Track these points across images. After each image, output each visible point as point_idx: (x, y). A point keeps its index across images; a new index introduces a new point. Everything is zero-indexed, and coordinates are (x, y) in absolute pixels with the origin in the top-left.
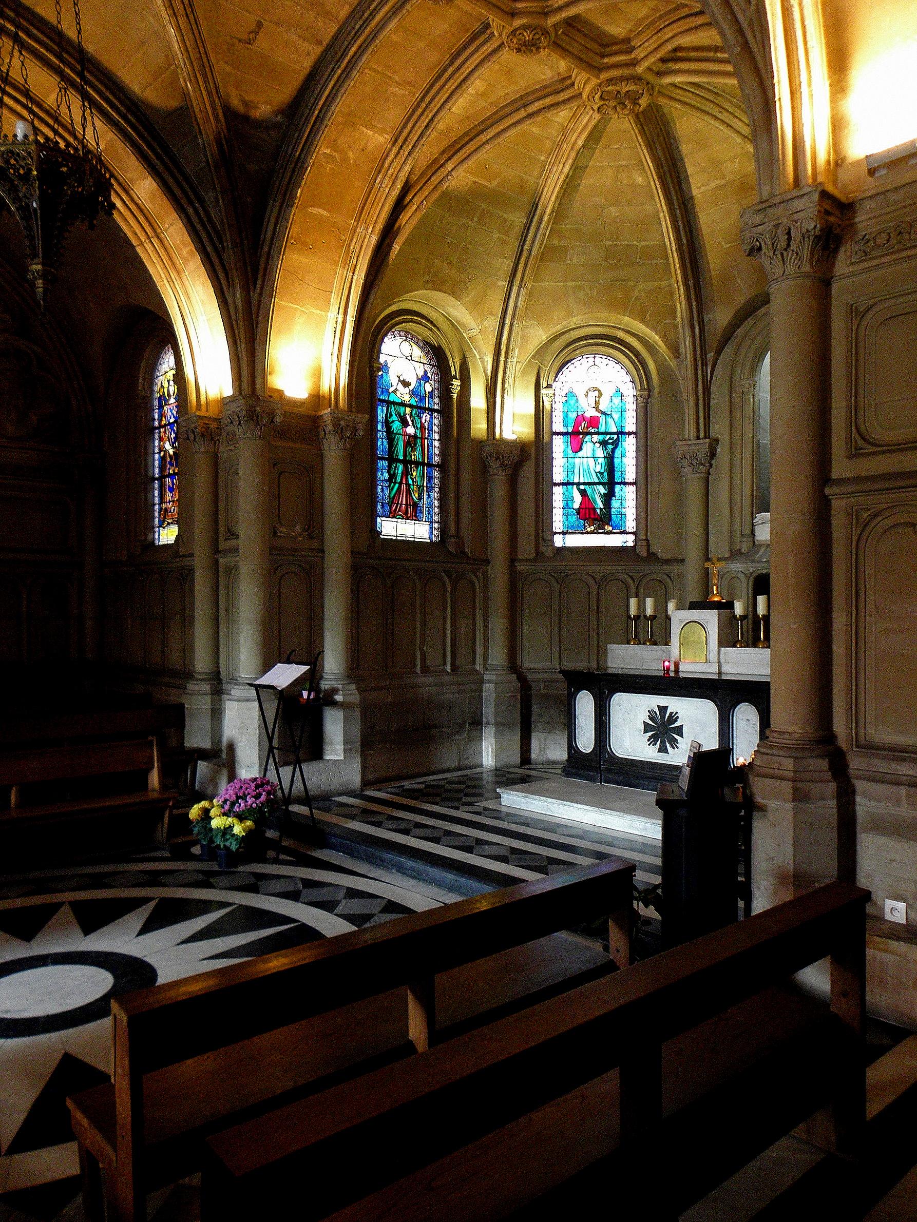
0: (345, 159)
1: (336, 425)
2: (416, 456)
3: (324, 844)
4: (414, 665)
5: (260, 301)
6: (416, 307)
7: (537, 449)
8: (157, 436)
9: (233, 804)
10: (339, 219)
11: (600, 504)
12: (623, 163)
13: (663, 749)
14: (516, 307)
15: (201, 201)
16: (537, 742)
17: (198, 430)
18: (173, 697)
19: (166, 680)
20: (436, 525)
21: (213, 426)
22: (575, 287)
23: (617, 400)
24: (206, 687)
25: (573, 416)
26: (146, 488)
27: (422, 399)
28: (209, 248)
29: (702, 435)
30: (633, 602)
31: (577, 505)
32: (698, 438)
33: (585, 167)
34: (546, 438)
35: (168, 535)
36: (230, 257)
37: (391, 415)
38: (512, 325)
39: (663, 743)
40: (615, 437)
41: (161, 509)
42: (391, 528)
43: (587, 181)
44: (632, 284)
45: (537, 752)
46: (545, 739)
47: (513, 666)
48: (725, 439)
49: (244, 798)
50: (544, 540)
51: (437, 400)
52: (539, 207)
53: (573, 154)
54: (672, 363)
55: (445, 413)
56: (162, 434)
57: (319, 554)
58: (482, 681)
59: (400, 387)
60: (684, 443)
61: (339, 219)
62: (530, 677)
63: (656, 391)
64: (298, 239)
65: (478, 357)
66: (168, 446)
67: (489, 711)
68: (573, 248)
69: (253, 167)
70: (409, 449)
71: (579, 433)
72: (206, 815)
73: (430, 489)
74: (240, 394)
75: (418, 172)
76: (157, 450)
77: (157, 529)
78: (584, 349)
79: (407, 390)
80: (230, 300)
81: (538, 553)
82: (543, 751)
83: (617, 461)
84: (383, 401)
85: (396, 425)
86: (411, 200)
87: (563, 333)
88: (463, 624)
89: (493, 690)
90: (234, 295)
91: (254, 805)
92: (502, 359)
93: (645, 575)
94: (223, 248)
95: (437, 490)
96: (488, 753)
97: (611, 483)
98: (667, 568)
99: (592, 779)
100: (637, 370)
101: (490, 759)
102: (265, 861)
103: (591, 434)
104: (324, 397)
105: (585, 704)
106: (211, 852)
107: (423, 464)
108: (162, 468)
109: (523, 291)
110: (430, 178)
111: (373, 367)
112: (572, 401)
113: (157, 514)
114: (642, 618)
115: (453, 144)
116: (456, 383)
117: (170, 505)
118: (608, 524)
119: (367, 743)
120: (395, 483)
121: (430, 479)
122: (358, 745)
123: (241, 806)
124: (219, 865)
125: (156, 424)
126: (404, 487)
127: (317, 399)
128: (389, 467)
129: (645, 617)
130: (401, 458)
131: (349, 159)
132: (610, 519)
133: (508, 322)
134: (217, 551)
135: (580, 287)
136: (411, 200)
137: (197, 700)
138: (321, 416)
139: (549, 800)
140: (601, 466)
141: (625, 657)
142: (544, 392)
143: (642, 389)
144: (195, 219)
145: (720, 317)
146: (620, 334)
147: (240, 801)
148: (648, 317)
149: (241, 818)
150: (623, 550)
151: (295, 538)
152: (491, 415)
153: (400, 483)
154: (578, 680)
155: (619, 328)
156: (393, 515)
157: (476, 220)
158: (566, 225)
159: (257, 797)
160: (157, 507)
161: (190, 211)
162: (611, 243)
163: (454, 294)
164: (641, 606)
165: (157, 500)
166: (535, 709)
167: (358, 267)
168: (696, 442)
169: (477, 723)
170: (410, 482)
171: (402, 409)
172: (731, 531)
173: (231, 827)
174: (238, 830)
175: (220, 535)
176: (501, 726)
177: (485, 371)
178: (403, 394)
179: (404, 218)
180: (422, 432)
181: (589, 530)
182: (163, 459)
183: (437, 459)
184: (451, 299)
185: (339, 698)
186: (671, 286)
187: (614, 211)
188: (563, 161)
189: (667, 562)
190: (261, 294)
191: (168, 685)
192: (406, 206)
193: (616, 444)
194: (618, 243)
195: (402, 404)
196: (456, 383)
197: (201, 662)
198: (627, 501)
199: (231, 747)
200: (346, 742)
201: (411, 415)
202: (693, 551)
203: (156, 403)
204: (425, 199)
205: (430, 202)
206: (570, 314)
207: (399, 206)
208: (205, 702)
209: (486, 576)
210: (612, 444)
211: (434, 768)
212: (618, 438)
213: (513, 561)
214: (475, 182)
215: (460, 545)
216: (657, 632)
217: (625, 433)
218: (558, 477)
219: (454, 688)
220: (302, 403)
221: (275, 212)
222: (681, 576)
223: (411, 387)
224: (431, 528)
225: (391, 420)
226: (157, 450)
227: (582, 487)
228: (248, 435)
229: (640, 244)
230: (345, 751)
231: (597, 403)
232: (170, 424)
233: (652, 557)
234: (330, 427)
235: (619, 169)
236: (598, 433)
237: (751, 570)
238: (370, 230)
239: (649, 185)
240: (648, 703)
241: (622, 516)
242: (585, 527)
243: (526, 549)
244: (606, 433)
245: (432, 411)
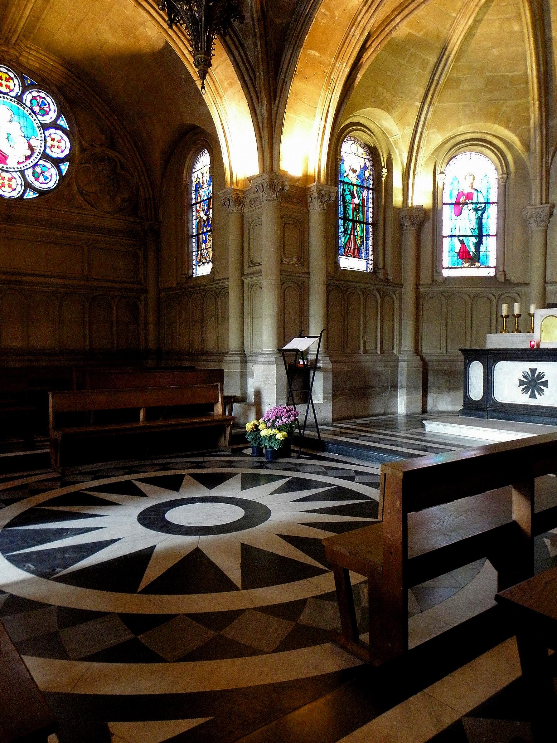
0: (333, 17)
1: (319, 193)
2: (359, 218)
3: (324, 450)
4: (359, 349)
5: (277, 111)
6: (361, 121)
7: (433, 213)
8: (194, 209)
9: (274, 422)
10: (325, 58)
11: (472, 249)
12: (507, 16)
13: (533, 396)
14: (425, 119)
15: (242, 46)
17: (233, 198)
18: (212, 366)
19: (204, 357)
20: (370, 262)
21: (241, 195)
24: (238, 359)
26: (188, 242)
27: (363, 181)
28: (246, 78)
29: (544, 202)
30: (505, 307)
31: (457, 250)
32: (542, 204)
33: (480, 21)
34: (439, 207)
35: (203, 270)
36: (261, 84)
37: (345, 191)
38: (422, 132)
39: (533, 392)
40: (483, 205)
41: (198, 255)
42: (347, 263)
43: (480, 31)
44: (502, 102)
45: (431, 405)
47: (417, 351)
49: (281, 418)
50: (437, 272)
51: (371, 182)
52: (448, 50)
53: (477, 10)
54: (524, 156)
55: (376, 190)
56: (198, 208)
57: (307, 276)
58: (397, 361)
59: (351, 173)
60: (531, 207)
61: (325, 58)
62: (427, 358)
63: (512, 176)
64: (300, 72)
65: (398, 154)
66: (202, 215)
67: (402, 379)
68: (465, 79)
69: (278, 21)
70: (355, 213)
71: (460, 204)
72: (256, 429)
73: (367, 239)
74: (264, 172)
75: (376, 26)
76: (194, 218)
77: (194, 267)
79: (355, 175)
80: (258, 111)
82: (435, 405)
83: (484, 221)
84: (341, 181)
85: (348, 198)
86: (371, 45)
87: (452, 138)
88: (387, 324)
89: (405, 366)
90: (262, 107)
91: (287, 422)
92: (414, 154)
94: (255, 78)
95: (371, 239)
96: (402, 405)
97: (480, 236)
98: (518, 289)
99: (482, 417)
100: (500, 161)
101: (403, 409)
102: (291, 457)
103: (467, 204)
104: (310, 176)
105: (476, 370)
106: (259, 452)
107: (363, 222)
108: (198, 229)
109: (431, 109)
110: (384, 29)
111: (337, 159)
112: (455, 183)
113: (194, 258)
114: (511, 316)
115: (400, 5)
116: (385, 170)
117: (203, 252)
118: (478, 262)
119: (337, 393)
120: (347, 234)
121: (368, 232)
122: (331, 395)
123: (279, 423)
124: (267, 458)
125: (194, 201)
126: (352, 237)
127: (306, 178)
128: (344, 223)
129: (514, 315)
130: (351, 218)
131: (335, 16)
132: (479, 259)
134: (243, 275)
136: (371, 45)
137: (231, 366)
138: (309, 188)
139: (461, 426)
142: (438, 177)
143: (503, 173)
144: (239, 59)
146: (489, 138)
147: (278, 420)
148: (510, 125)
149: (280, 431)
150: (488, 278)
151: (293, 265)
152: (405, 192)
153: (350, 234)
154: (472, 355)
155: (489, 134)
156: (346, 254)
157: (406, 60)
158: (462, 63)
159: (289, 417)
160: (194, 254)
161: (236, 53)
162: (491, 74)
163: (388, 111)
164: (511, 308)
165: (194, 249)
166: (430, 378)
167: (335, 90)
168: (541, 206)
169: (395, 386)
170: (356, 234)
171: (351, 187)
173: (274, 435)
174: (280, 436)
175: (247, 265)
176: (410, 389)
177: (402, 163)
178: (352, 178)
179: (365, 57)
180: (363, 202)
181: (465, 265)
182: (199, 223)
183: (371, 220)
184: (386, 114)
185: (320, 365)
186: (528, 102)
187: (496, 52)
188: (468, 16)
189: (518, 285)
190: (278, 107)
191: (207, 361)
192: (367, 49)
193: (484, 210)
194: (496, 74)
195: (352, 184)
196: (385, 170)
197: (233, 343)
198: (490, 247)
199: (258, 394)
200: (324, 393)
201: (357, 191)
202: (536, 279)
203: (194, 188)
204: (380, 43)
205: (383, 46)
206: (459, 124)
207: (363, 49)
208: (237, 368)
209: (401, 294)
210: (481, 210)
211: (371, 413)
212: (485, 207)
213: (417, 285)
214: (409, 33)
215: (386, 273)
216: (525, 324)
218: (446, 231)
219: (382, 364)
220: (298, 180)
221: (290, 52)
223: (357, 173)
224: (367, 264)
225: (345, 194)
226: (194, 218)
227: (461, 238)
228: (269, 198)
229: (511, 74)
230: (324, 398)
231: (472, 184)
232: (203, 201)
233: (508, 282)
234: (316, 195)
235: (503, 21)
236: (473, 203)
238: (344, 65)
239: (522, 32)
240: (521, 368)
241: (487, 257)
242: (462, 264)
243: (426, 278)
244: (477, 203)
245: (368, 189)
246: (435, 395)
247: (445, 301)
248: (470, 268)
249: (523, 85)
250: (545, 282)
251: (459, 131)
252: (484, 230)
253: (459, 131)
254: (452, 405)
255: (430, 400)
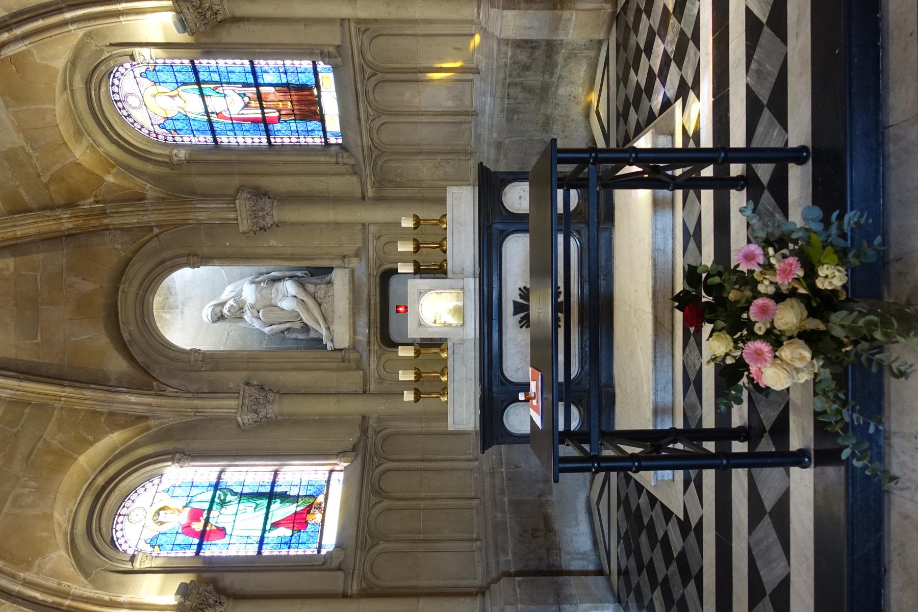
16: (574, 563)
22: (13, 505)
23: (178, 491)
25: (182, 539)
31: (289, 532)
45: (585, 563)
46: (569, 554)
48: (243, 375)
50: (323, 564)
62: (494, 575)
78: (103, 522)
81: (340, 569)
82: (583, 556)
93: (376, 454)
112: (162, 540)
133: (17, 588)
135: (18, 497)
140: (248, 506)
141: (463, 410)
142: (137, 566)
145: (116, 364)
146: (101, 481)
148: (90, 437)
168: (241, 397)
172: (338, 369)
186: (62, 408)
189: (364, 431)
202: (356, 406)
210: (226, 495)
217: (217, 484)
222: (380, 420)
227: (268, 527)
237: (377, 348)
244: (212, 501)
246: (565, 557)
247: (382, 546)
248: (325, 510)
249: (27, 410)
250: (365, 392)
251: (64, 525)
252: (262, 490)
253: (64, 525)
254: (577, 525)
255: (576, 565)
